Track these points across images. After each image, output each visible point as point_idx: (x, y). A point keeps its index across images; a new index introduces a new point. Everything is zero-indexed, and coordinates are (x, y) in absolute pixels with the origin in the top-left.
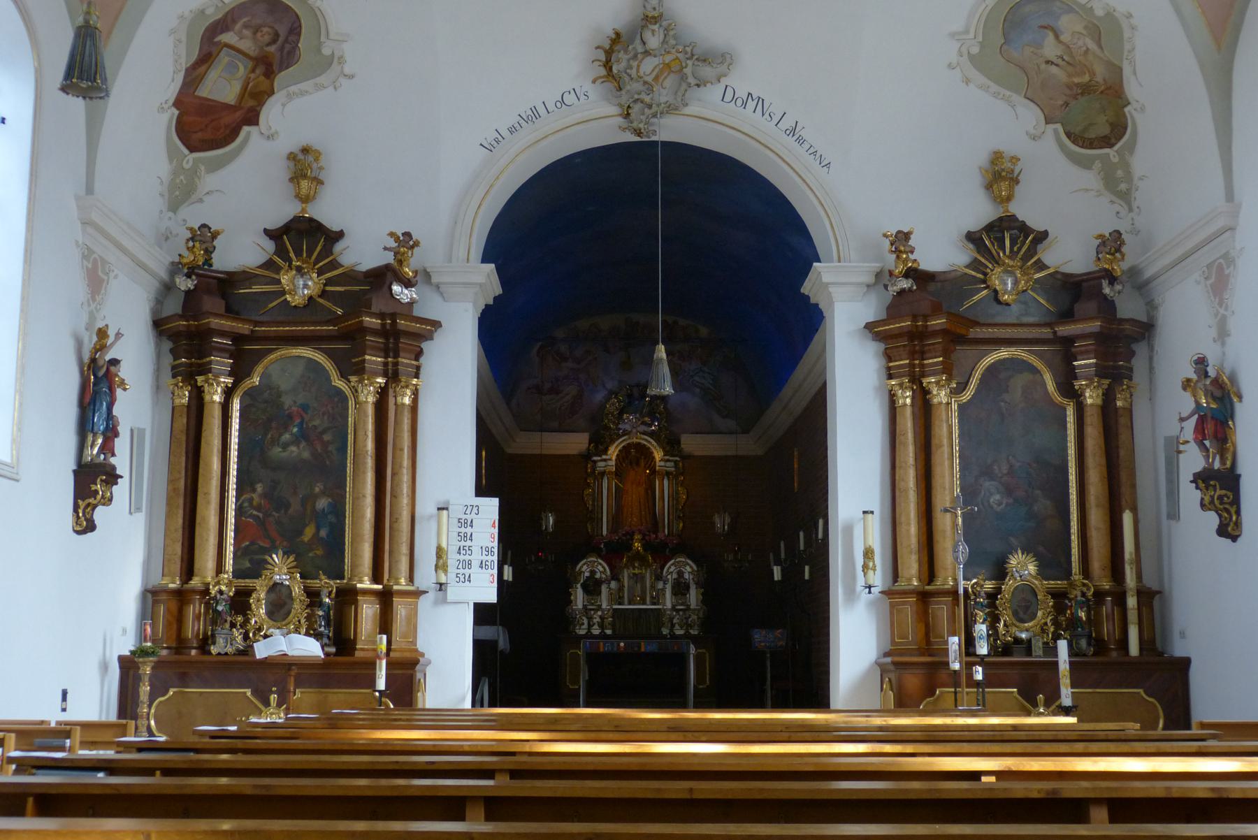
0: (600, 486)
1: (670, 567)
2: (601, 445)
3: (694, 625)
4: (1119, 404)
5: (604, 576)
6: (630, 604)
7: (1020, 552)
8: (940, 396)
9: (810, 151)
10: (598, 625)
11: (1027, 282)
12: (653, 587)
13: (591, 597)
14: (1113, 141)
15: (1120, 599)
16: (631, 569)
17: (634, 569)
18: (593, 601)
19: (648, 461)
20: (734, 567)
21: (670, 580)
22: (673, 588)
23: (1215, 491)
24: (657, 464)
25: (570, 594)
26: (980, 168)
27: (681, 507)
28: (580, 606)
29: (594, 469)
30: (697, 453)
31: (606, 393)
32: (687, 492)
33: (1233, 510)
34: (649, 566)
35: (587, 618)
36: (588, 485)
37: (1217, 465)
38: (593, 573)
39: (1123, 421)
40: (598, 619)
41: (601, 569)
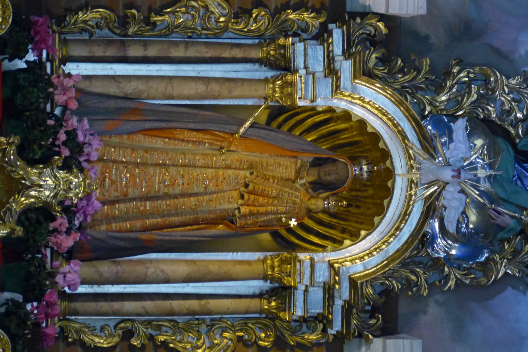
0: (238, 53)
2: (381, 60)
19: (320, 222)
24: (318, 256)
27: (162, 338)
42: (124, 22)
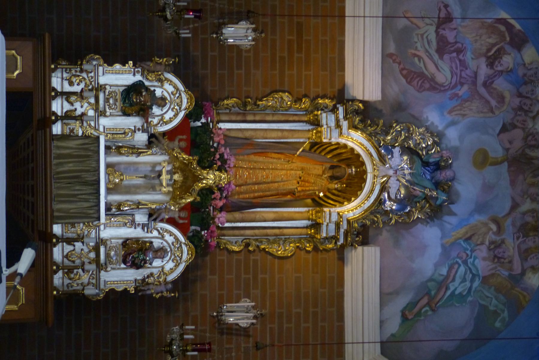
0: (296, 118)
1: (171, 234)
2: (361, 121)
3: (70, 279)
5: (155, 121)
6: (108, 166)
10: (71, 111)
12: (138, 205)
13: (119, 97)
16: (169, 168)
17: (168, 172)
18: (111, 101)
19: (334, 194)
20: (171, 344)
21: (150, 235)
22: (137, 240)
24: (333, 210)
27: (263, 247)
28: (102, 80)
29: (324, 108)
30: (348, 270)
31: (440, 128)
32: (287, 258)
34: (174, 198)
35: (82, 90)
36: (298, 100)
38: (162, 102)
40: (79, 112)
41: (167, 117)
42: (245, 104)
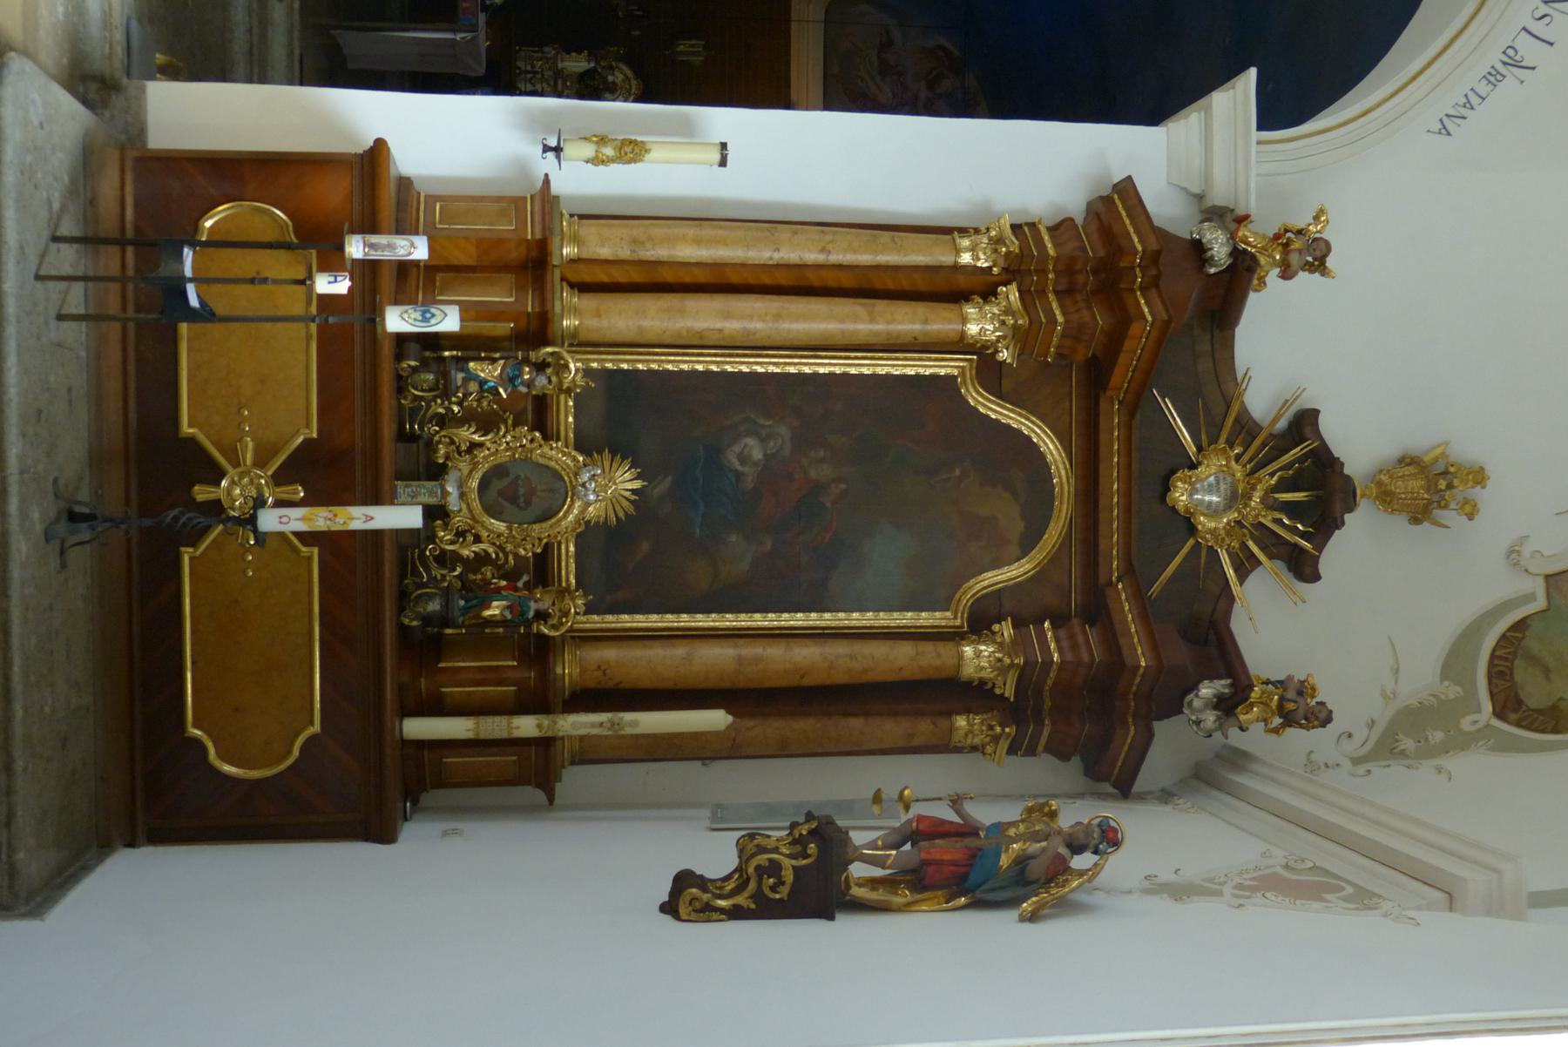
4: (961, 722)
7: (637, 485)
8: (979, 323)
9: (1473, 97)
11: (1213, 532)
14: (1513, 716)
15: (537, 701)
23: (791, 856)
25: (579, 52)
26: (1447, 443)
33: (741, 900)
37: (858, 870)
39: (924, 728)
